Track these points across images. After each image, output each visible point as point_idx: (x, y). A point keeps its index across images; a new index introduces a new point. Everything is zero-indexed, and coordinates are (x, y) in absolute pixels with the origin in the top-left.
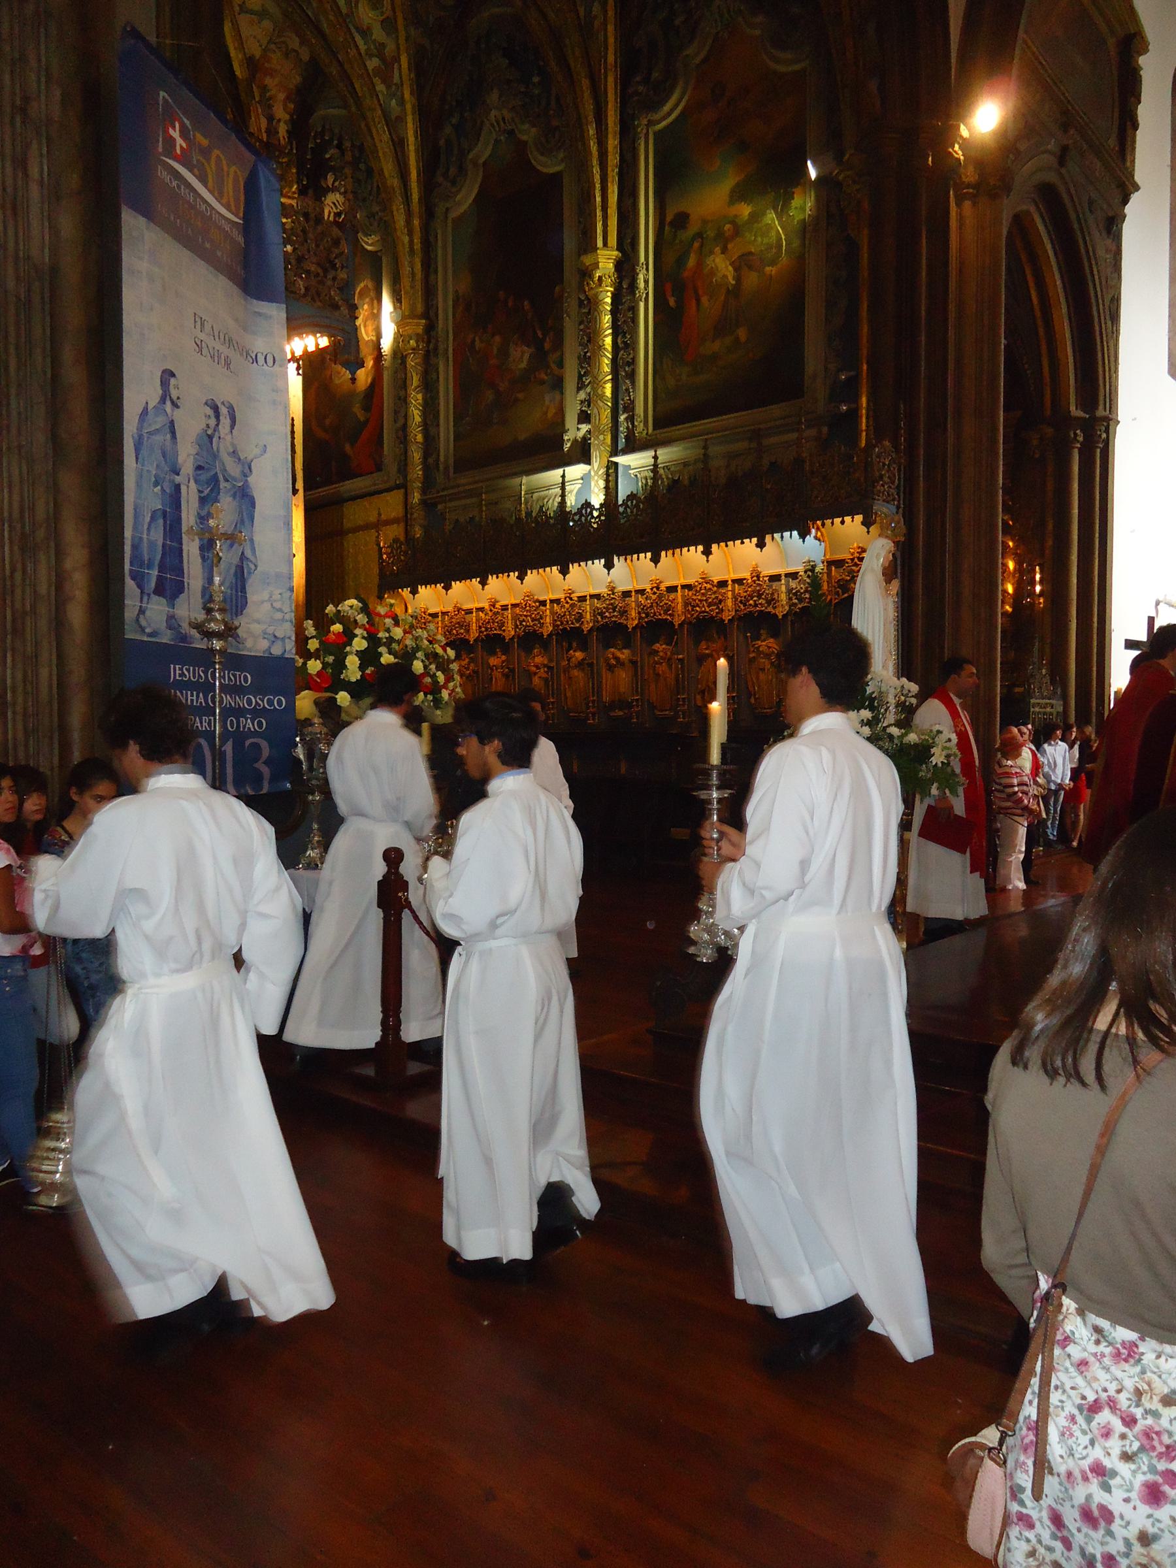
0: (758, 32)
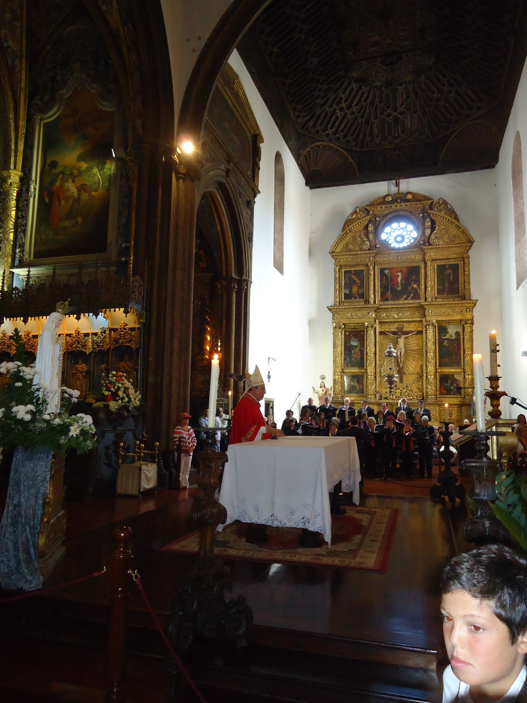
0: (94, 91)
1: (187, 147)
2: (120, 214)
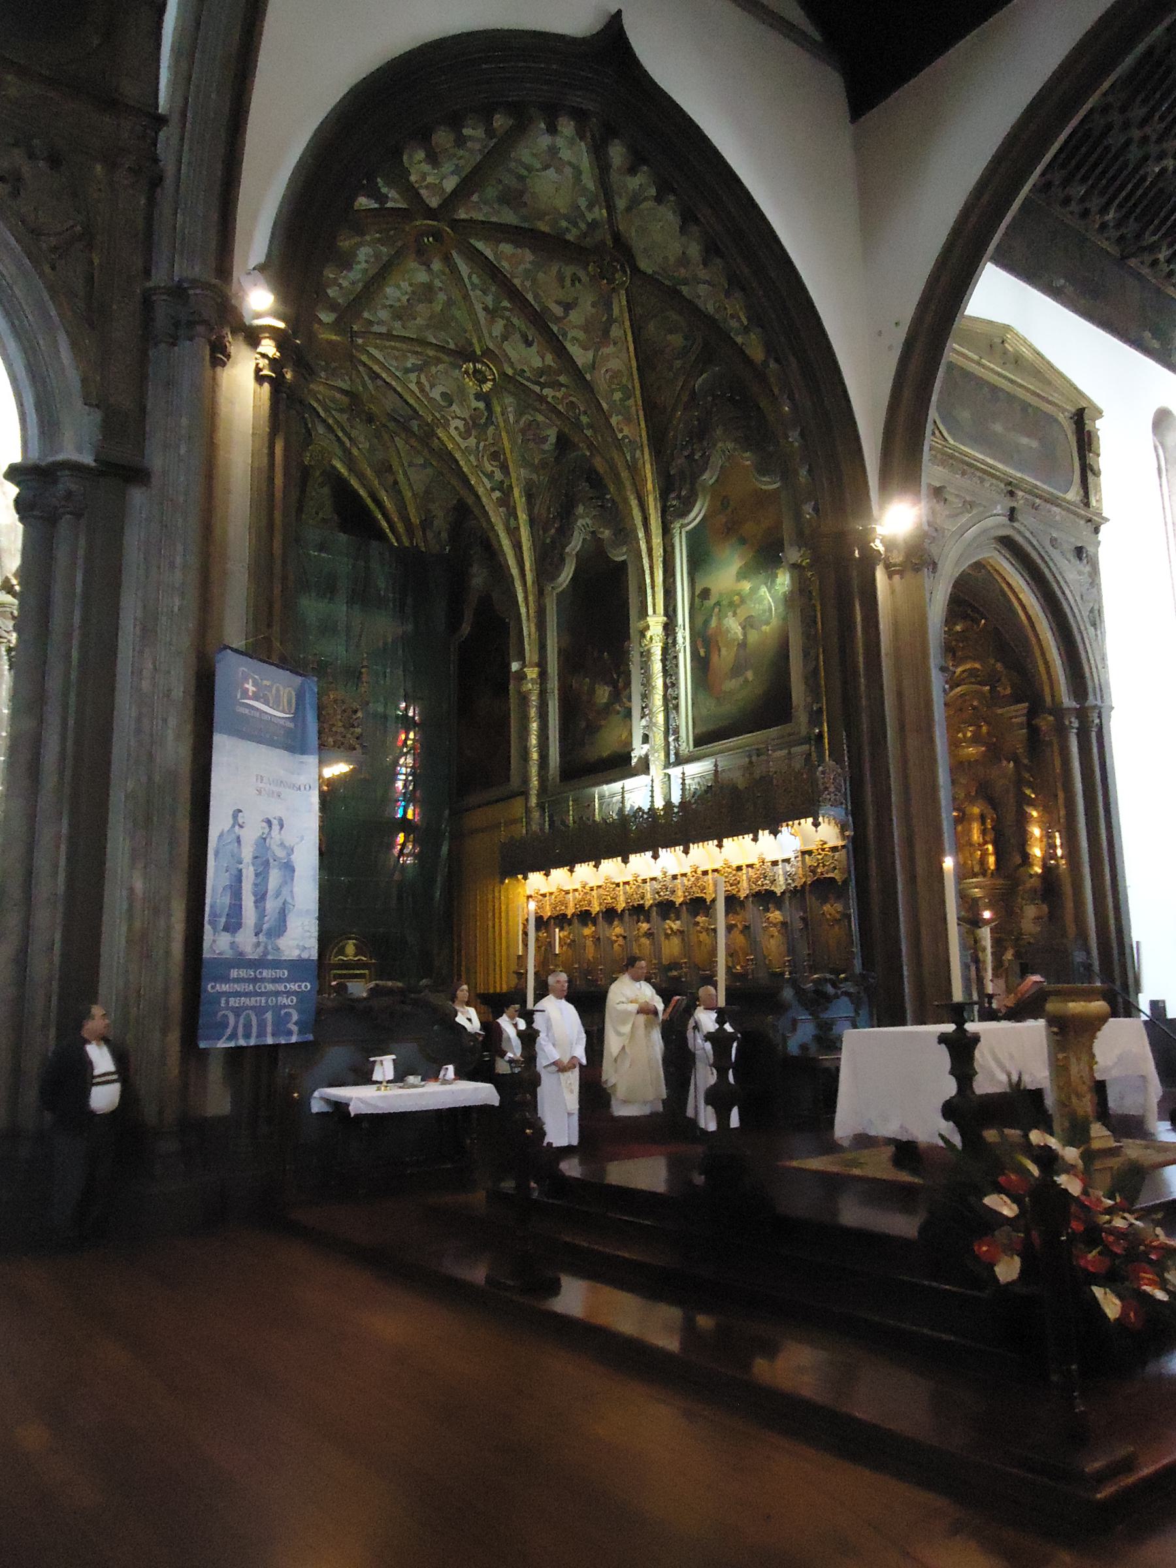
0: (748, 463)
1: (896, 520)
2: (806, 655)
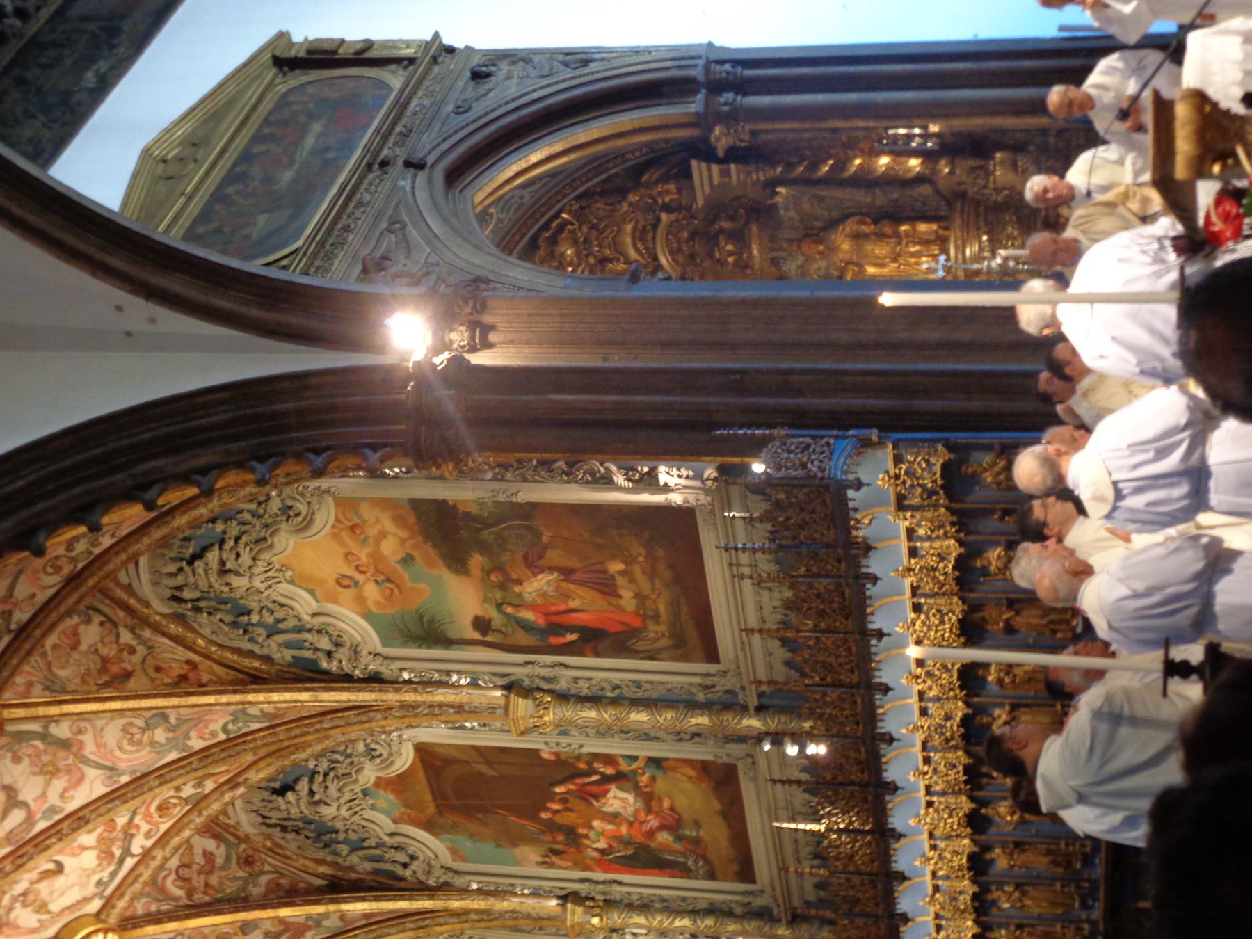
0: (291, 543)
1: (409, 335)
